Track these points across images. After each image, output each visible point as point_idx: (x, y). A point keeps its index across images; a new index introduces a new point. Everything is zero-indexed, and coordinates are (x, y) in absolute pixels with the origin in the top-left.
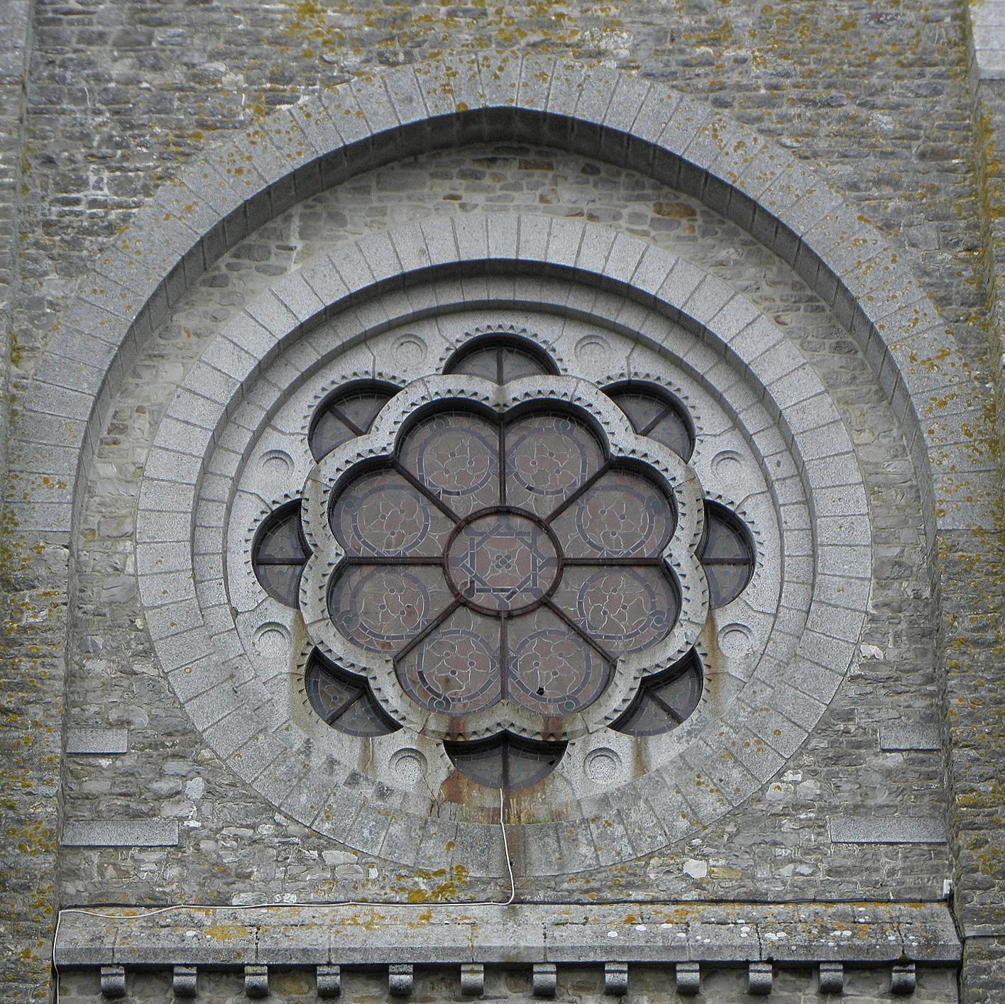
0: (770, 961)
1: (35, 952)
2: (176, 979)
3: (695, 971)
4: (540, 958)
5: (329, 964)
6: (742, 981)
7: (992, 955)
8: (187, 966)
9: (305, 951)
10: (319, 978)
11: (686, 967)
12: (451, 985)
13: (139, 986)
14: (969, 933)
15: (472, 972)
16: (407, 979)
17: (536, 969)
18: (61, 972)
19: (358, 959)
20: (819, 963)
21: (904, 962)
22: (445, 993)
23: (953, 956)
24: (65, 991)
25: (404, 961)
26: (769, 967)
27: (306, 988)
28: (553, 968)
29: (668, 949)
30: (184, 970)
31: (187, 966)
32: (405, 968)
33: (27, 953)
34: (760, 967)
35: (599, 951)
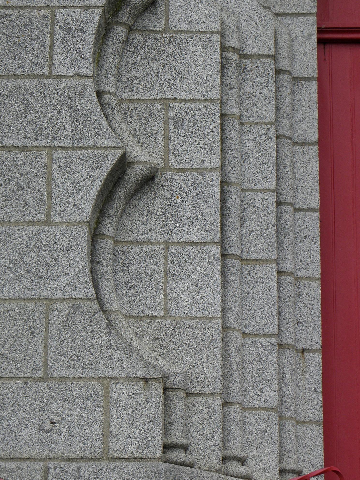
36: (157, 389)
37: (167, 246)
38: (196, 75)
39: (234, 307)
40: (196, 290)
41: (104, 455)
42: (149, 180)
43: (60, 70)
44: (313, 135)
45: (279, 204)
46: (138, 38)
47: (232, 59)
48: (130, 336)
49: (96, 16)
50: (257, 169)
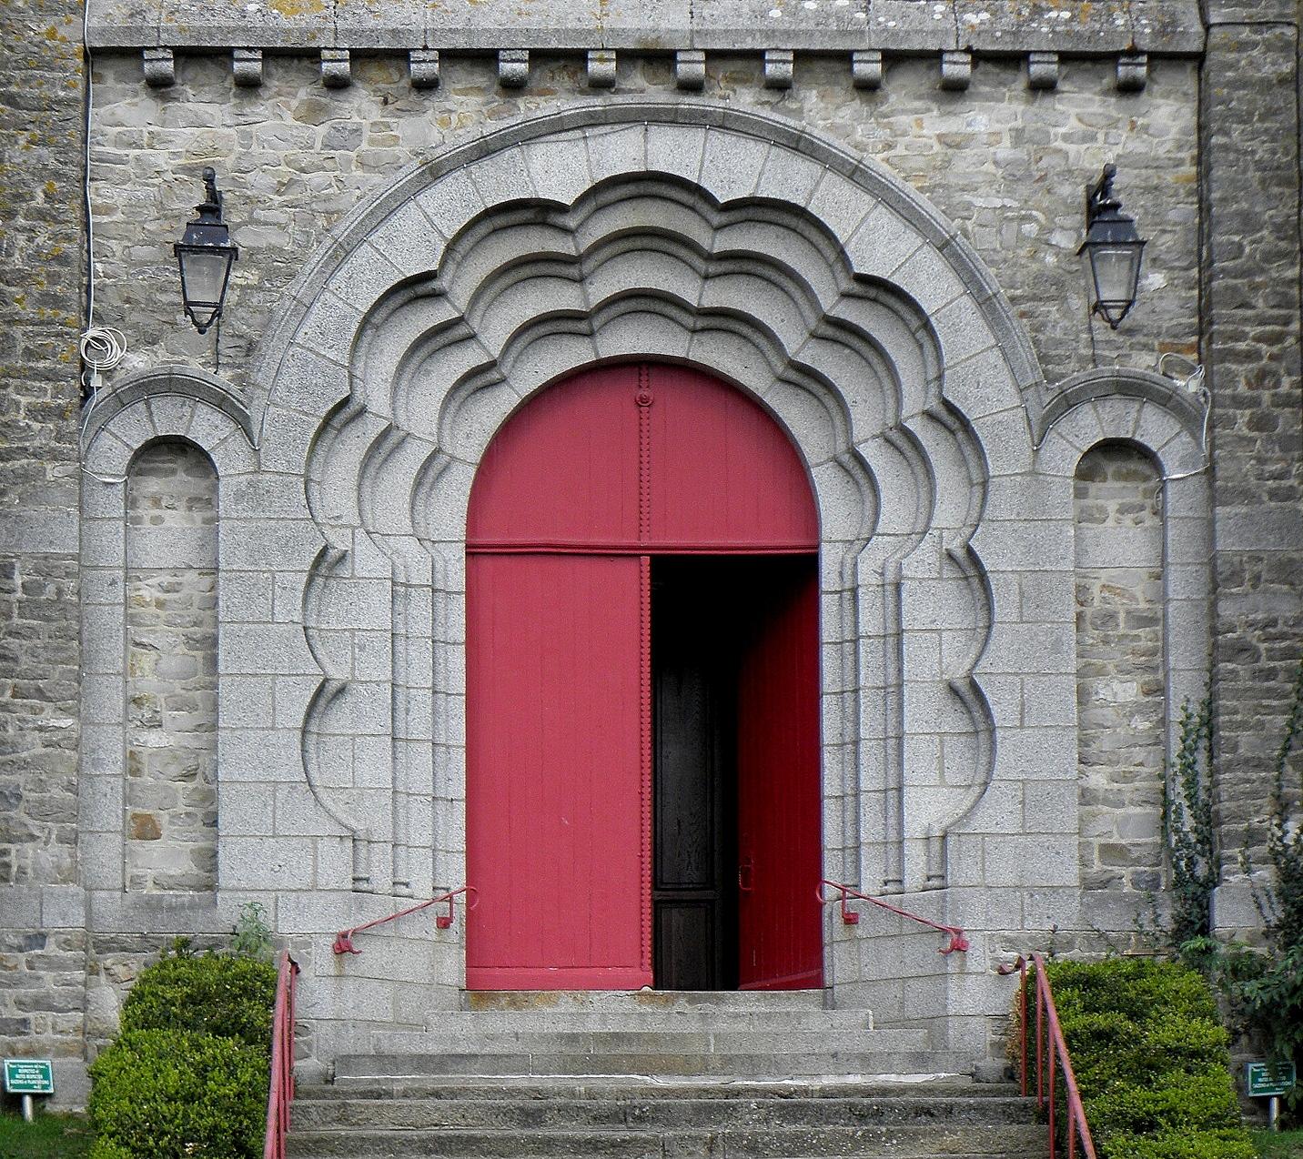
0: (968, 50)
1: (62, 32)
2: (236, 66)
3: (877, 62)
4: (686, 44)
5: (425, 48)
6: (933, 74)
7: (1242, 46)
8: (249, 49)
9: (395, 32)
10: (413, 66)
11: (865, 57)
12: (575, 73)
13: (190, 73)
14: (1214, 19)
15: (601, 60)
16: (522, 68)
17: (680, 57)
18: (93, 56)
19: (461, 43)
20: (1029, 53)
21: (1133, 53)
22: (568, 83)
23: (1194, 46)
24: (99, 78)
25: (518, 47)
26: (968, 58)
27: (396, 77)
28: (701, 56)
29: (843, 33)
30: (246, 54)
31: (249, 49)
32: (519, 55)
33: (52, 34)
34: (956, 57)
35: (758, 35)
36: (349, 844)
37: (354, 737)
38: (374, 610)
39: (401, 776)
40: (374, 767)
41: (314, 888)
42: (342, 690)
43: (279, 618)
44: (462, 638)
45: (435, 692)
46: (333, 582)
47: (399, 590)
48: (328, 803)
49: (304, 577)
50: (418, 674)
